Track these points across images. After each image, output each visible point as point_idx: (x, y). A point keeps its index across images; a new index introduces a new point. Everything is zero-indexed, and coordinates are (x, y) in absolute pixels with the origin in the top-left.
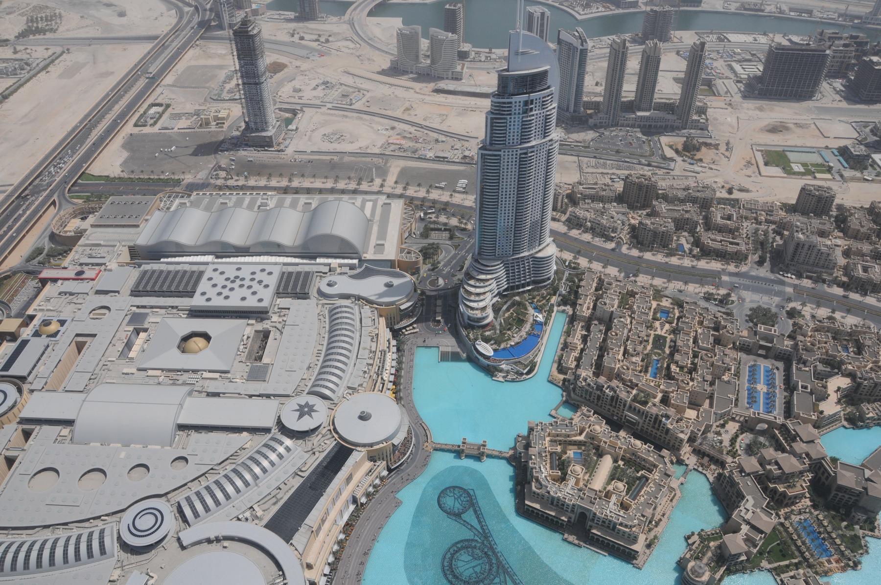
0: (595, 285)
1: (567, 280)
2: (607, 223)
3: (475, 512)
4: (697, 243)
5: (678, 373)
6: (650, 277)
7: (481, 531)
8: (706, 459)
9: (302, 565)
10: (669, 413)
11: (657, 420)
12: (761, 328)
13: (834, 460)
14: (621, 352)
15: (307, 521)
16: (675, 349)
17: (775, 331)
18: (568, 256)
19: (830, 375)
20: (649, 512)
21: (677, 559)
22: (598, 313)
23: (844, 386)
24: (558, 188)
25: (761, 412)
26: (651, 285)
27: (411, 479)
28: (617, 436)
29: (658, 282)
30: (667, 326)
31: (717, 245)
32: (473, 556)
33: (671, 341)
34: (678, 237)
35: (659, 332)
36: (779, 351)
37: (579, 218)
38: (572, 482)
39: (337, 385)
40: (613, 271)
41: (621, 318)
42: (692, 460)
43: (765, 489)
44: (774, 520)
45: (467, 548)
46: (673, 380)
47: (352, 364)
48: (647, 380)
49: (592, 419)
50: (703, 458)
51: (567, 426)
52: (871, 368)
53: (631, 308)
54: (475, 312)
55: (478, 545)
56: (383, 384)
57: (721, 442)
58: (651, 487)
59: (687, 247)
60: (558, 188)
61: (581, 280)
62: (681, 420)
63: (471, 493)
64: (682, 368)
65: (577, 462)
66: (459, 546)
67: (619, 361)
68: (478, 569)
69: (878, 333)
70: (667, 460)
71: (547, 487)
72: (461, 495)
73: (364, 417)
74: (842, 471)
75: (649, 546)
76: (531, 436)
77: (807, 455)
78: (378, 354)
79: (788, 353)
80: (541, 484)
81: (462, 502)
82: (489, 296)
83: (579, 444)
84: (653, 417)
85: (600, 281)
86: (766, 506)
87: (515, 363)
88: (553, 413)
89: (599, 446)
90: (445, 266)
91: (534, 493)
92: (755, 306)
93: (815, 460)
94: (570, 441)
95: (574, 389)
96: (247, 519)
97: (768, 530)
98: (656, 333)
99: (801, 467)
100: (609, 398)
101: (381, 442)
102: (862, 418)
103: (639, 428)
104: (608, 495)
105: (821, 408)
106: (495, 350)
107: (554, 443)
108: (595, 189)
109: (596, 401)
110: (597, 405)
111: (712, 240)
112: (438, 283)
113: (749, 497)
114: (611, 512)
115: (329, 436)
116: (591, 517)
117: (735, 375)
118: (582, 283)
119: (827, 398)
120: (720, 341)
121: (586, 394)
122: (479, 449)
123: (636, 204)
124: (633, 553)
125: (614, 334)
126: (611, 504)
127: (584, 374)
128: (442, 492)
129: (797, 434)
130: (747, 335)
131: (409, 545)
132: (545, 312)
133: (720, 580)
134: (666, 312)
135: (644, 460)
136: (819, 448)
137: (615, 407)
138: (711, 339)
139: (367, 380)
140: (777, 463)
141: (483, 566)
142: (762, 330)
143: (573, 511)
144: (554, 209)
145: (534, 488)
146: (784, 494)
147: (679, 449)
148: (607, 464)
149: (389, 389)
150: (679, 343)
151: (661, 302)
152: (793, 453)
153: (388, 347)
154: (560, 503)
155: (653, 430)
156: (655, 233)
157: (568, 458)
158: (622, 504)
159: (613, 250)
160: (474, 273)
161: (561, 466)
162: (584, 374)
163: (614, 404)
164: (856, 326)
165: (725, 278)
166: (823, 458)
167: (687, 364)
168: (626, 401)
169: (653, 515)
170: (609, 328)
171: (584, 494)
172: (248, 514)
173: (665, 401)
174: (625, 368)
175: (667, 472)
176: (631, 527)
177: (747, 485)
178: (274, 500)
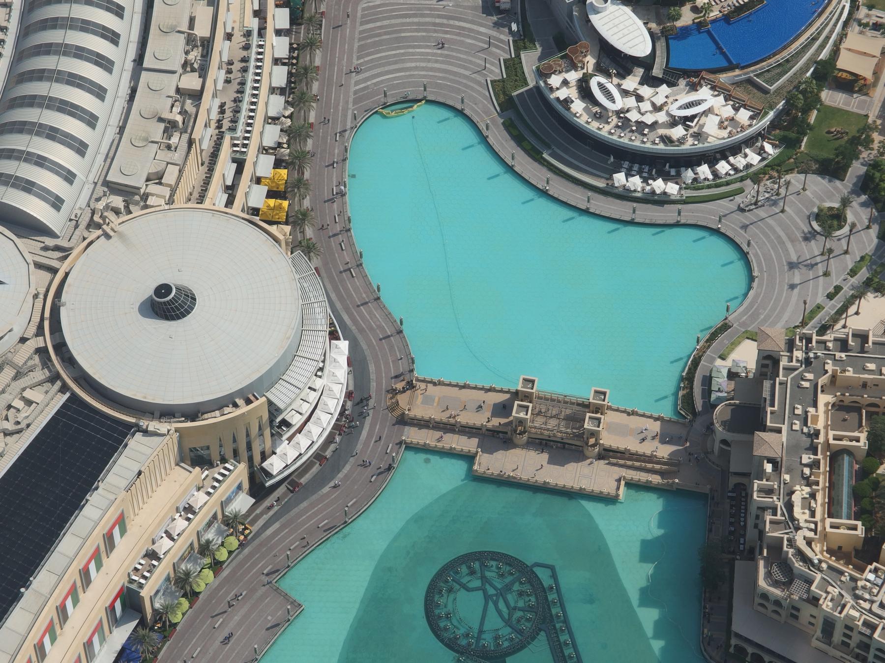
39: (69, 177)
47: (124, 90)
71: (810, 582)
72: (508, 588)
76: (767, 384)
78: (222, 50)
81: (512, 610)
91: (765, 596)
101: (230, 401)
107: (852, 417)
115: (40, 374)
122: (576, 420)
128: (441, 575)
139: (178, 157)
145: (762, 583)
149: (258, 181)
154: (856, 639)
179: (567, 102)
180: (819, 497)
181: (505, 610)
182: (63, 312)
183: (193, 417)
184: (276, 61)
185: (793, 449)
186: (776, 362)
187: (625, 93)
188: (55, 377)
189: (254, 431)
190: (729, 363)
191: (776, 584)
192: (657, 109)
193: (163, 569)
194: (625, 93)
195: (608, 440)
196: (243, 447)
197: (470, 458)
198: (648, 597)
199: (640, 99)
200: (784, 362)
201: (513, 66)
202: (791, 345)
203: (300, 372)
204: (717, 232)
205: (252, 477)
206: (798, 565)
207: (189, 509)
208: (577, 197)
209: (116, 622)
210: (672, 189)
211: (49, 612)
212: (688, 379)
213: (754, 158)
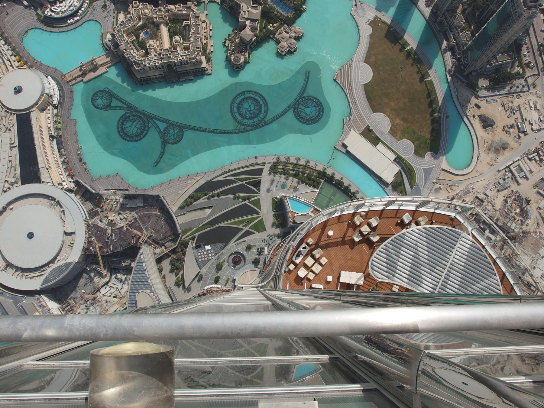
3: (116, 98)
7: (125, 106)
9: (57, 187)
15: (40, 166)
20: (199, 43)
21: (224, 59)
27: (72, 104)
28: (160, 10)
32: (131, 121)
38: (153, 52)
44: (259, 8)
45: (125, 119)
49: (141, 7)
51: (129, 20)
56: (9, 60)
63: (106, 90)
66: (121, 121)
68: (138, 126)
70: (192, 8)
73: (18, 90)
75: (208, 60)
76: (115, 39)
80: (138, 64)
81: (106, 98)
83: (142, 28)
86: (253, 4)
91: (138, 70)
96: (9, 188)
97: (259, 17)
101: (40, 98)
104: (175, 48)
114: (181, 56)
115: (9, 115)
122: (92, 64)
131: (98, 138)
133: (249, 57)
135: (181, 15)
141: (139, 122)
143: (163, 67)
145: (136, 68)
148: (164, 31)
149: (14, 61)
154: (154, 67)
157: (142, 39)
158: (184, 48)
161: (142, 45)
169: (202, 43)
171: (163, 55)
172: (7, 185)
178: (13, 169)
179: (51, 15)
182: (3, 103)
185: (126, 46)
186: (114, 34)
187: (58, 7)
188: (11, 114)
189: (48, 100)
190: (107, 39)
191: (138, 67)
192: (65, 6)
193: (52, 129)
194: (58, 7)
195: (100, 63)
197: (82, 81)
198: (123, 82)
199: (61, 6)
200: (115, 34)
201: (38, 14)
202: (114, 30)
203: (47, 86)
204: (90, 20)
205: (53, 106)
206: (139, 62)
207: (48, 118)
208: (65, 29)
209: (52, 141)
210: (78, 18)
211: (42, 147)
212: (104, 46)
213: (86, 4)
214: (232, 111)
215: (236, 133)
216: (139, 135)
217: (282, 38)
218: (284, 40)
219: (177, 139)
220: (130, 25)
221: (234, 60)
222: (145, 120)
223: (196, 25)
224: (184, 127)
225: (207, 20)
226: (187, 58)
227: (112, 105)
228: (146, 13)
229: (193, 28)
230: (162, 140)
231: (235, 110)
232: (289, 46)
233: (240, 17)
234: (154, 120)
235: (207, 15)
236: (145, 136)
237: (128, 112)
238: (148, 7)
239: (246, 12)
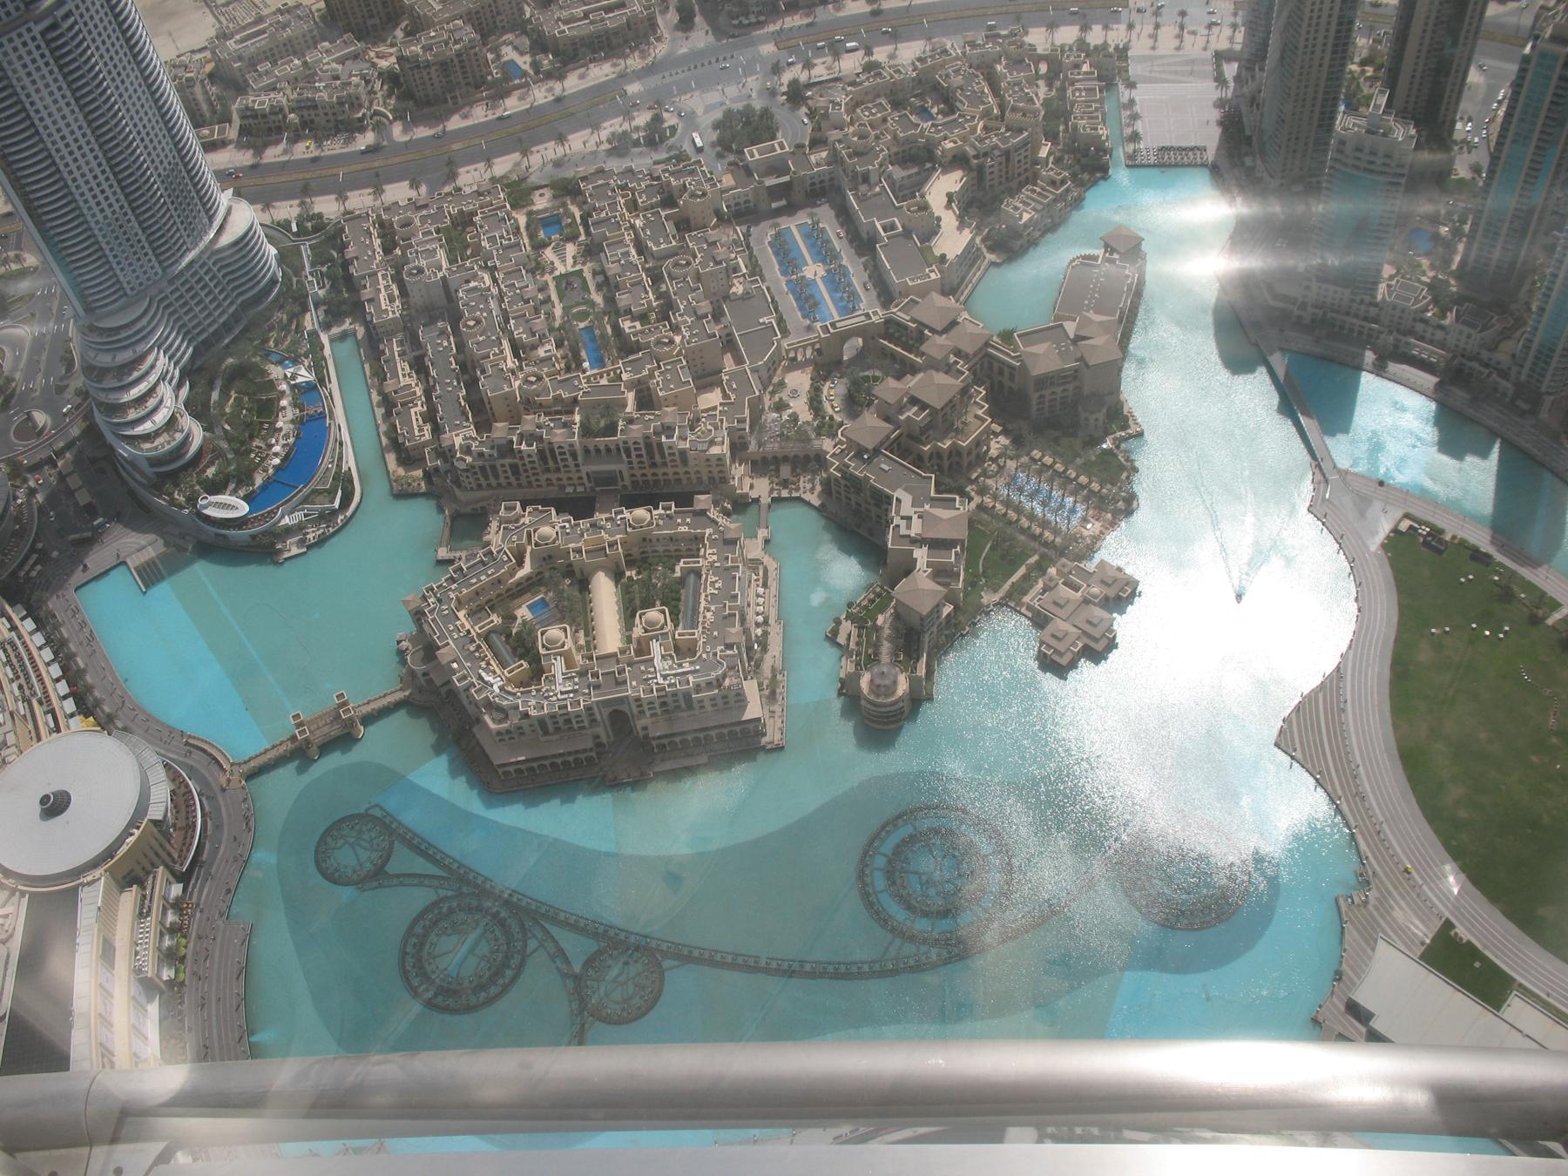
0: (377, 242)
1: (313, 265)
2: (331, 96)
4: (540, 44)
5: (642, 332)
6: (481, 166)
8: (785, 471)
10: (668, 420)
11: (651, 449)
12: (754, 154)
13: (1007, 336)
14: (508, 352)
16: (609, 286)
17: (782, 148)
18: (287, 210)
19: (926, 179)
20: (737, 628)
22: (417, 298)
23: (957, 187)
24: (181, 72)
25: (837, 318)
26: (493, 180)
29: (503, 166)
30: (571, 249)
31: (582, 29)
33: (595, 274)
34: (496, 50)
35: (561, 269)
36: (809, 182)
37: (264, 116)
38: (558, 667)
40: (399, 192)
41: (468, 282)
42: (761, 488)
43: (919, 461)
45: (435, 923)
46: (639, 350)
48: (590, 377)
49: (526, 520)
50: (777, 471)
51: (482, 561)
52: (985, 128)
53: (478, 250)
54: (157, 442)
55: (454, 904)
56: (53, 712)
57: (794, 418)
58: (713, 583)
59: (524, 62)
60: (181, 72)
61: (344, 246)
62: (698, 420)
63: (377, 813)
64: (643, 318)
65: (549, 623)
66: (419, 930)
67: (513, 372)
68: (484, 948)
69: (964, 53)
70: (713, 513)
73: (54, 806)
74: (1029, 349)
75: (772, 697)
76: (426, 627)
77: (958, 353)
79: (827, 177)
80: (499, 709)
82: (166, 390)
84: (642, 446)
85: (386, 230)
86: (937, 491)
87: (306, 500)
88: (443, 553)
89: (570, 565)
90: (29, 377)
91: (499, 733)
92: (718, 115)
93: (975, 355)
94: (509, 590)
95: (457, 483)
97: (962, 533)
98: (557, 273)
99: (958, 383)
100: (535, 458)
101: (126, 833)
102: (1015, 233)
103: (627, 482)
104: (643, 649)
105: (937, 253)
106: (246, 498)
108: (263, 32)
109: (512, 479)
110: (520, 485)
111: (566, 22)
112: (35, 426)
113: (899, 493)
114: (665, 677)
116: (635, 710)
117: (752, 274)
118: (351, 252)
119: (939, 226)
120: (687, 221)
121: (487, 478)
123: (370, 22)
124: (751, 726)
125: (472, 323)
126: (657, 662)
127: (458, 441)
129: (921, 324)
130: (732, 183)
132: (307, 357)
134: (552, 221)
136: (970, 328)
137: (558, 470)
138: (670, 228)
140: (914, 401)
142: (757, 156)
143: (593, 721)
144: (198, 122)
145: (492, 726)
146: (955, 451)
147: (724, 480)
148: (605, 592)
150: (612, 269)
151: (533, 203)
152: (933, 365)
153: (14, 628)
154: (561, 720)
155: (655, 471)
156: (444, 66)
157: (524, 623)
158: (677, 649)
159: (372, 150)
160: (105, 360)
161: (523, 647)
162: (458, 441)
163: (551, 464)
164: (920, 59)
165: (633, 88)
166: (987, 344)
167: (649, 302)
168: (571, 445)
169: (746, 632)
170: (456, 318)
171: (595, 675)
173: (646, 401)
174: (533, 379)
175: (728, 536)
176: (719, 683)
177: (880, 473)
180: (492, 662)
181: (367, 845)
183: (112, 858)
184: (31, 633)
188: (13, 891)
191: (500, 722)
196: (155, 859)
202: (424, 598)
214: (865, 885)
215: (883, 974)
216: (482, 987)
217: (1055, 603)
218: (1063, 613)
219: (637, 1001)
220: (483, 578)
221: (871, 690)
222: (515, 928)
223: (727, 569)
224: (666, 955)
225: (767, 560)
226: (688, 683)
227: (392, 868)
228: (542, 538)
229: (712, 585)
230: (575, 1005)
231: (880, 882)
232: (1084, 632)
233: (890, 537)
234: (547, 926)
235: (767, 542)
236: (506, 988)
237: (450, 893)
238: (554, 518)
239: (915, 517)
